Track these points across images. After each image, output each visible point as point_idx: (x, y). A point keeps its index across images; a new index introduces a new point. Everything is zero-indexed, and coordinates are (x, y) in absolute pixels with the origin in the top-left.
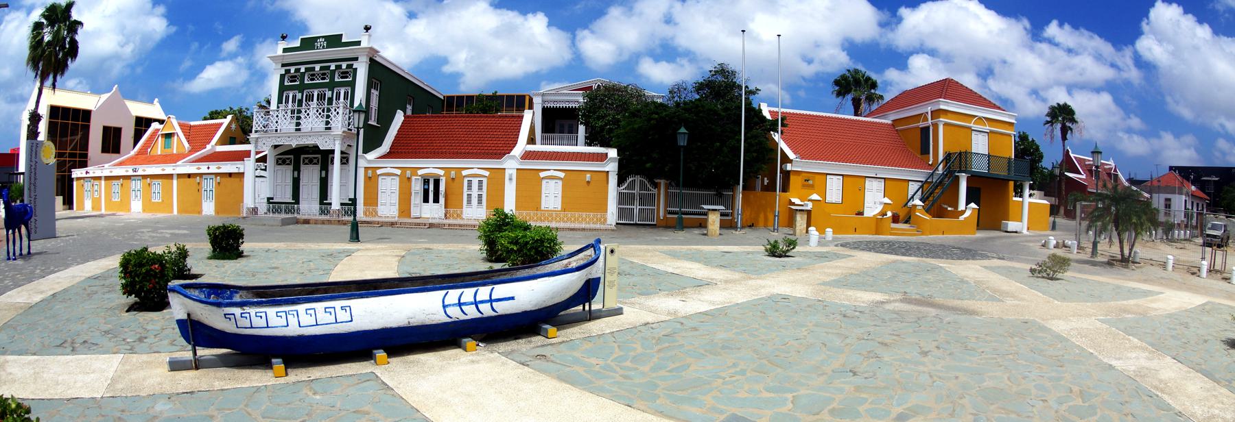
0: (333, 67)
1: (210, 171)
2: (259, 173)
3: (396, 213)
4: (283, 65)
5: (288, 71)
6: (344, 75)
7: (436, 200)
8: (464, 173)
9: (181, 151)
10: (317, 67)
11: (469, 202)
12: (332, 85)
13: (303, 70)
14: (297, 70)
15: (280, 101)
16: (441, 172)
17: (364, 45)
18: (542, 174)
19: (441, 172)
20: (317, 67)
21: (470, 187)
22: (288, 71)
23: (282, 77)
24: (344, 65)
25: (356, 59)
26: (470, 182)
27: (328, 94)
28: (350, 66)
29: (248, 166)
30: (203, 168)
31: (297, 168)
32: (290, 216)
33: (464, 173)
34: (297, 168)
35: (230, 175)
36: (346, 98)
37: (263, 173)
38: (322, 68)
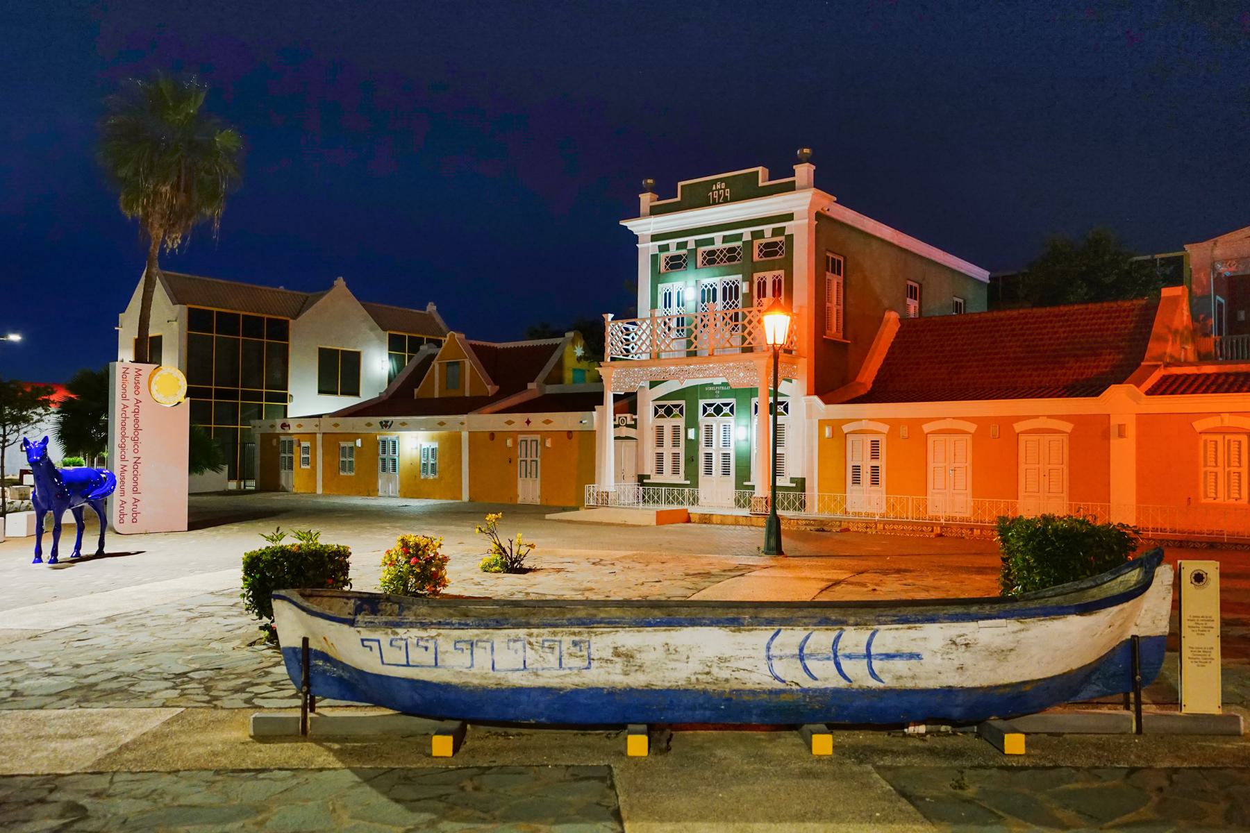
0: (747, 237)
1: (532, 427)
2: (625, 432)
6: (770, 249)
9: (480, 393)
10: (717, 236)
13: (691, 246)
18: (1199, 425)
27: (744, 288)
29: (605, 418)
30: (518, 419)
31: (692, 422)
32: (675, 507)
35: (570, 434)
37: (631, 432)
38: (725, 240)
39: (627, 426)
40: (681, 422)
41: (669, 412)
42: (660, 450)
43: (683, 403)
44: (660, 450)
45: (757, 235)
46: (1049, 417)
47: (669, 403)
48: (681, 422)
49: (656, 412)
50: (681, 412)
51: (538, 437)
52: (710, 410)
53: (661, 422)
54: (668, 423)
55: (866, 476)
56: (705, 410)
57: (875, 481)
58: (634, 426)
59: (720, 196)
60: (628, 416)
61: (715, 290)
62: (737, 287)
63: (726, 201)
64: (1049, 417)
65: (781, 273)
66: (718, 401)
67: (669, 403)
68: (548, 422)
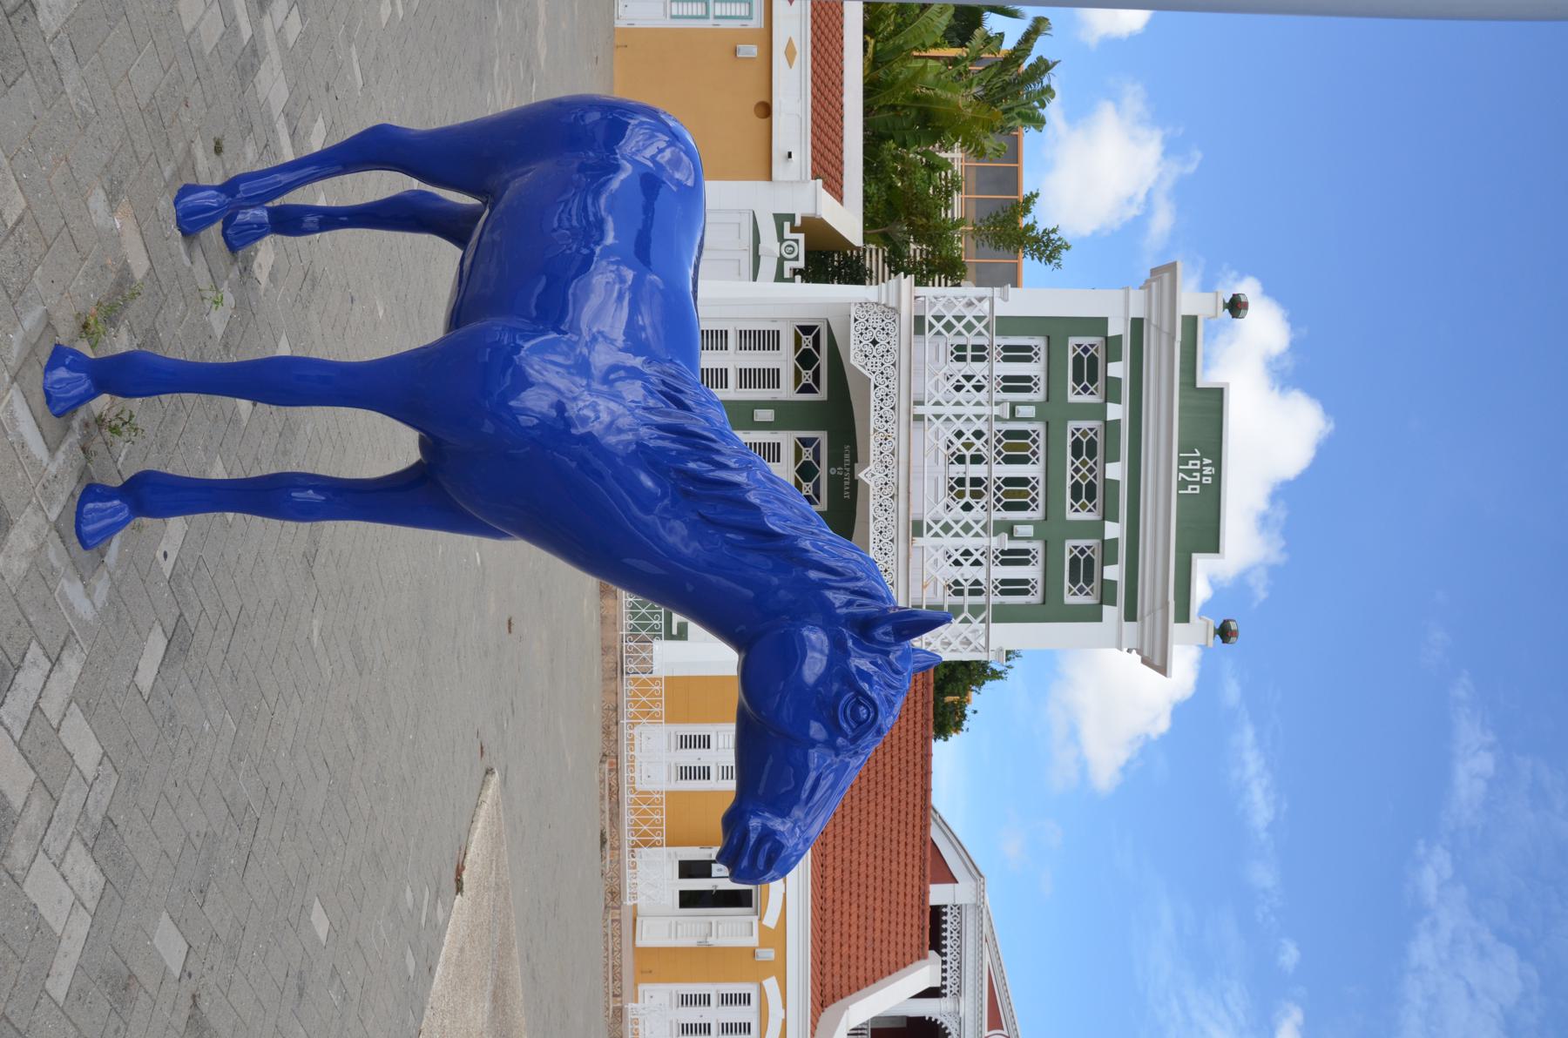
0: (1113, 530)
3: (642, 786)
4: (1137, 325)
5: (1112, 348)
6: (1083, 570)
7: (689, 900)
8: (771, 984)
11: (686, 1000)
12: (1052, 530)
14: (1112, 391)
15: (1007, 325)
16: (771, 920)
17: (1176, 629)
19: (771, 920)
20: (1116, 471)
21: (727, 1000)
22: (1112, 348)
23: (1097, 325)
24: (1114, 572)
25: (1131, 615)
26: (745, 999)
28: (1107, 593)
33: (771, 984)
34: (787, 416)
35: (766, 110)
36: (1012, 587)
37: (768, 266)
38: (1111, 486)
39: (781, 260)
40: (786, 391)
41: (806, 359)
42: (732, 340)
43: (822, 394)
44: (732, 340)
45: (1109, 551)
46: (785, 1022)
47: (823, 360)
48: (786, 391)
49: (806, 330)
50: (806, 389)
51: (757, 22)
52: (807, 454)
53: (787, 341)
54: (783, 360)
55: (693, 757)
56: (806, 442)
57: (687, 773)
58: (780, 277)
59: (1189, 472)
60: (801, 264)
61: (1024, 460)
62: (1024, 507)
63: (1183, 484)
64: (785, 1022)
65: (1034, 598)
66: (823, 472)
67: (823, 360)
68: (790, 53)
